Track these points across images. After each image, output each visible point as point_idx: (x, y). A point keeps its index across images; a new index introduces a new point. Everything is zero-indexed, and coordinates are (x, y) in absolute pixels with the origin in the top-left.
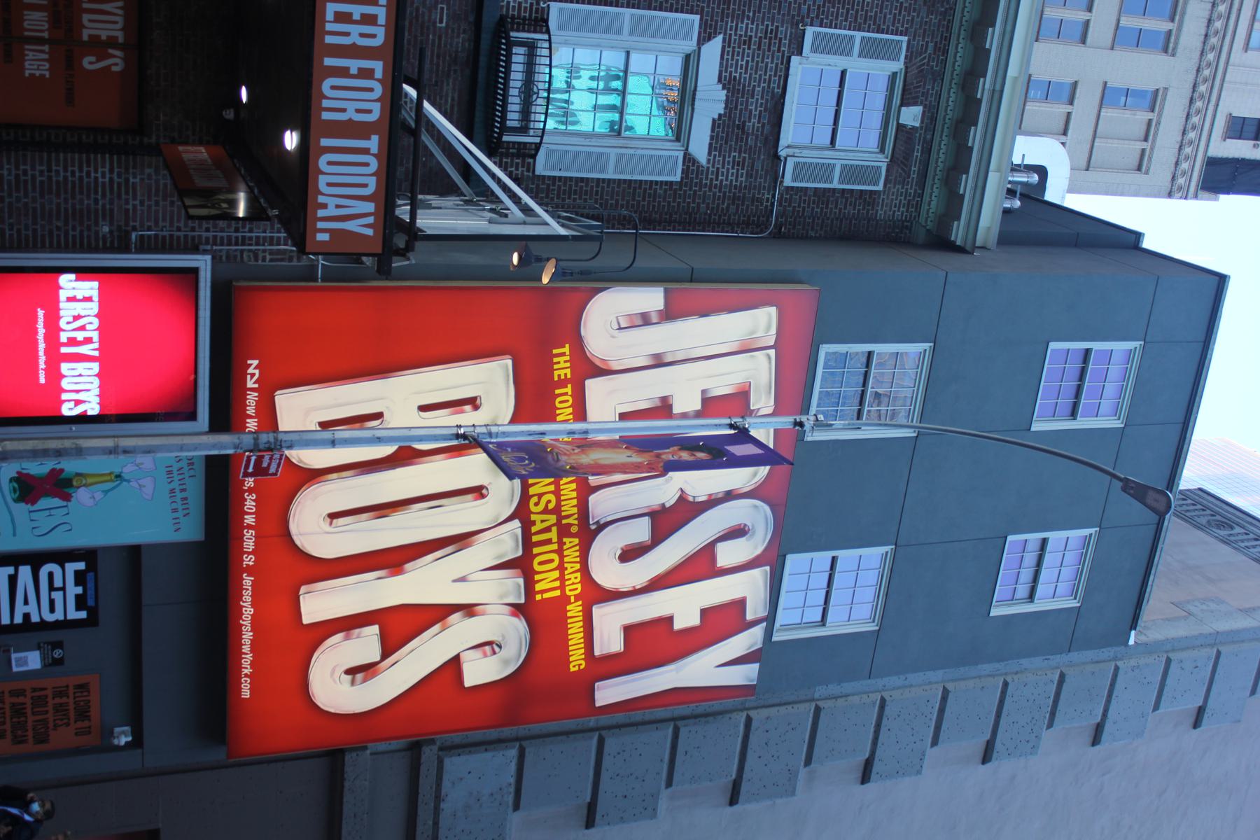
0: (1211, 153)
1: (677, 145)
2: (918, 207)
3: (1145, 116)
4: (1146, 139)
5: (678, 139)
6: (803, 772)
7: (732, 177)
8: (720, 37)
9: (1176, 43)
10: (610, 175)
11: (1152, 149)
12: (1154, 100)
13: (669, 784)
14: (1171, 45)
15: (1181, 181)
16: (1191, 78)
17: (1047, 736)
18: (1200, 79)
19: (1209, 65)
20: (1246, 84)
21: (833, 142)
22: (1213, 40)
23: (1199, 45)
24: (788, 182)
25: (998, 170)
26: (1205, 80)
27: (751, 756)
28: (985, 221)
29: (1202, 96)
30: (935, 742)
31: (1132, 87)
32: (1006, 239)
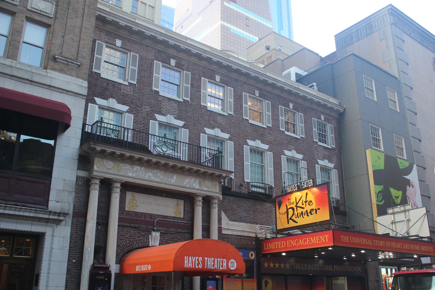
1: (332, 170)
2: (334, 117)
5: (331, 170)
6: (421, 154)
7: (335, 159)
8: (318, 160)
10: (338, 185)
13: (424, 182)
17: (413, 100)
21: (123, 67)
24: (334, 146)
25: (329, 99)
27: (420, 165)
28: (336, 103)
30: (415, 125)
32: (335, 97)
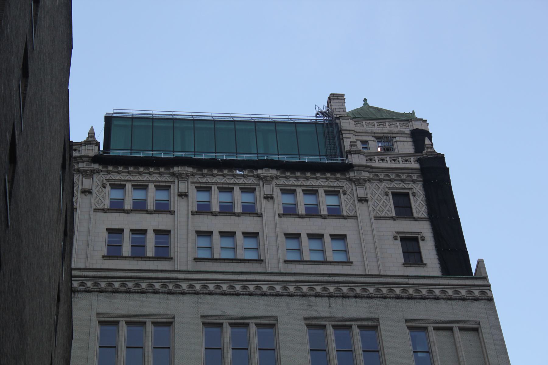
0: (437, 272)
3: (433, 336)
4: (451, 329)
9: (368, 320)
11: (457, 322)
12: (417, 328)
14: (370, 324)
15: (477, 293)
16: (392, 302)
18: (391, 295)
19: (378, 290)
20: (377, 257)
22: (358, 290)
23: (364, 301)
26: (391, 290)
29: (404, 290)
31: (411, 349)
